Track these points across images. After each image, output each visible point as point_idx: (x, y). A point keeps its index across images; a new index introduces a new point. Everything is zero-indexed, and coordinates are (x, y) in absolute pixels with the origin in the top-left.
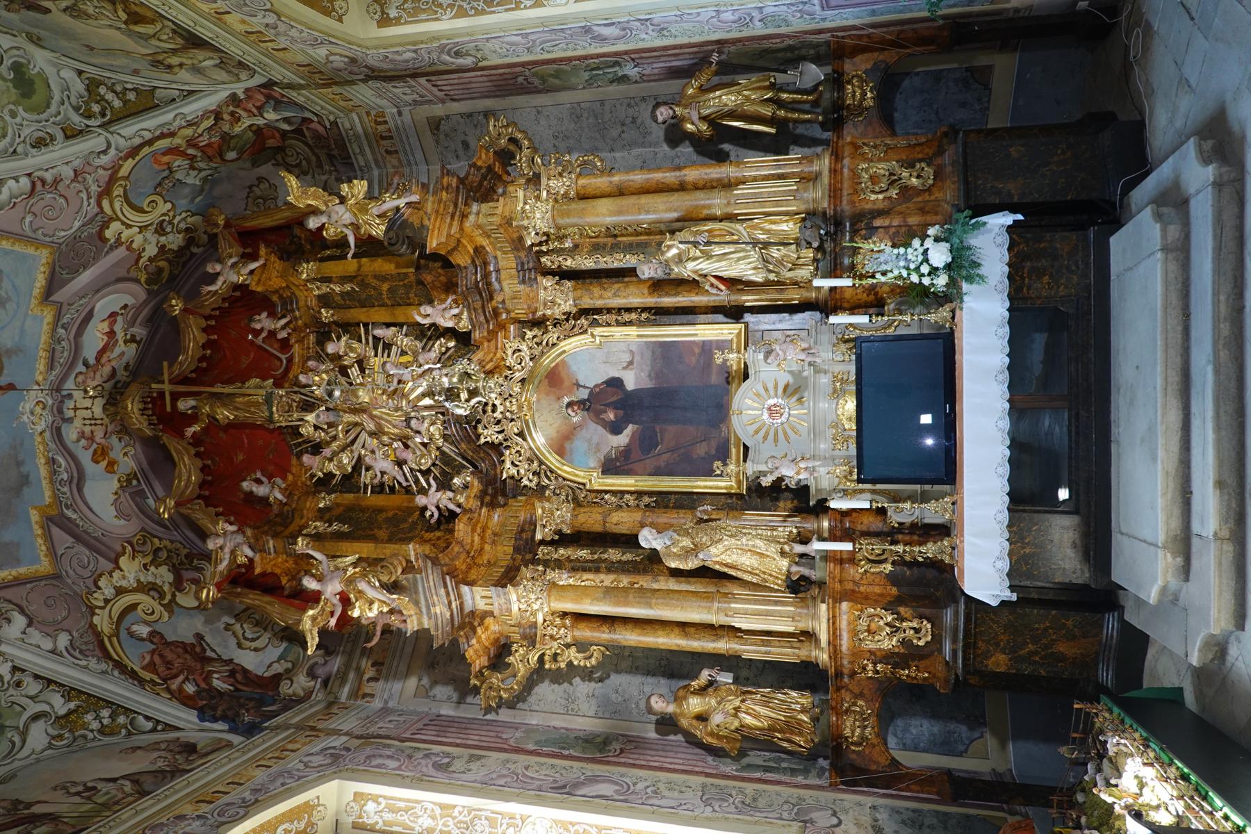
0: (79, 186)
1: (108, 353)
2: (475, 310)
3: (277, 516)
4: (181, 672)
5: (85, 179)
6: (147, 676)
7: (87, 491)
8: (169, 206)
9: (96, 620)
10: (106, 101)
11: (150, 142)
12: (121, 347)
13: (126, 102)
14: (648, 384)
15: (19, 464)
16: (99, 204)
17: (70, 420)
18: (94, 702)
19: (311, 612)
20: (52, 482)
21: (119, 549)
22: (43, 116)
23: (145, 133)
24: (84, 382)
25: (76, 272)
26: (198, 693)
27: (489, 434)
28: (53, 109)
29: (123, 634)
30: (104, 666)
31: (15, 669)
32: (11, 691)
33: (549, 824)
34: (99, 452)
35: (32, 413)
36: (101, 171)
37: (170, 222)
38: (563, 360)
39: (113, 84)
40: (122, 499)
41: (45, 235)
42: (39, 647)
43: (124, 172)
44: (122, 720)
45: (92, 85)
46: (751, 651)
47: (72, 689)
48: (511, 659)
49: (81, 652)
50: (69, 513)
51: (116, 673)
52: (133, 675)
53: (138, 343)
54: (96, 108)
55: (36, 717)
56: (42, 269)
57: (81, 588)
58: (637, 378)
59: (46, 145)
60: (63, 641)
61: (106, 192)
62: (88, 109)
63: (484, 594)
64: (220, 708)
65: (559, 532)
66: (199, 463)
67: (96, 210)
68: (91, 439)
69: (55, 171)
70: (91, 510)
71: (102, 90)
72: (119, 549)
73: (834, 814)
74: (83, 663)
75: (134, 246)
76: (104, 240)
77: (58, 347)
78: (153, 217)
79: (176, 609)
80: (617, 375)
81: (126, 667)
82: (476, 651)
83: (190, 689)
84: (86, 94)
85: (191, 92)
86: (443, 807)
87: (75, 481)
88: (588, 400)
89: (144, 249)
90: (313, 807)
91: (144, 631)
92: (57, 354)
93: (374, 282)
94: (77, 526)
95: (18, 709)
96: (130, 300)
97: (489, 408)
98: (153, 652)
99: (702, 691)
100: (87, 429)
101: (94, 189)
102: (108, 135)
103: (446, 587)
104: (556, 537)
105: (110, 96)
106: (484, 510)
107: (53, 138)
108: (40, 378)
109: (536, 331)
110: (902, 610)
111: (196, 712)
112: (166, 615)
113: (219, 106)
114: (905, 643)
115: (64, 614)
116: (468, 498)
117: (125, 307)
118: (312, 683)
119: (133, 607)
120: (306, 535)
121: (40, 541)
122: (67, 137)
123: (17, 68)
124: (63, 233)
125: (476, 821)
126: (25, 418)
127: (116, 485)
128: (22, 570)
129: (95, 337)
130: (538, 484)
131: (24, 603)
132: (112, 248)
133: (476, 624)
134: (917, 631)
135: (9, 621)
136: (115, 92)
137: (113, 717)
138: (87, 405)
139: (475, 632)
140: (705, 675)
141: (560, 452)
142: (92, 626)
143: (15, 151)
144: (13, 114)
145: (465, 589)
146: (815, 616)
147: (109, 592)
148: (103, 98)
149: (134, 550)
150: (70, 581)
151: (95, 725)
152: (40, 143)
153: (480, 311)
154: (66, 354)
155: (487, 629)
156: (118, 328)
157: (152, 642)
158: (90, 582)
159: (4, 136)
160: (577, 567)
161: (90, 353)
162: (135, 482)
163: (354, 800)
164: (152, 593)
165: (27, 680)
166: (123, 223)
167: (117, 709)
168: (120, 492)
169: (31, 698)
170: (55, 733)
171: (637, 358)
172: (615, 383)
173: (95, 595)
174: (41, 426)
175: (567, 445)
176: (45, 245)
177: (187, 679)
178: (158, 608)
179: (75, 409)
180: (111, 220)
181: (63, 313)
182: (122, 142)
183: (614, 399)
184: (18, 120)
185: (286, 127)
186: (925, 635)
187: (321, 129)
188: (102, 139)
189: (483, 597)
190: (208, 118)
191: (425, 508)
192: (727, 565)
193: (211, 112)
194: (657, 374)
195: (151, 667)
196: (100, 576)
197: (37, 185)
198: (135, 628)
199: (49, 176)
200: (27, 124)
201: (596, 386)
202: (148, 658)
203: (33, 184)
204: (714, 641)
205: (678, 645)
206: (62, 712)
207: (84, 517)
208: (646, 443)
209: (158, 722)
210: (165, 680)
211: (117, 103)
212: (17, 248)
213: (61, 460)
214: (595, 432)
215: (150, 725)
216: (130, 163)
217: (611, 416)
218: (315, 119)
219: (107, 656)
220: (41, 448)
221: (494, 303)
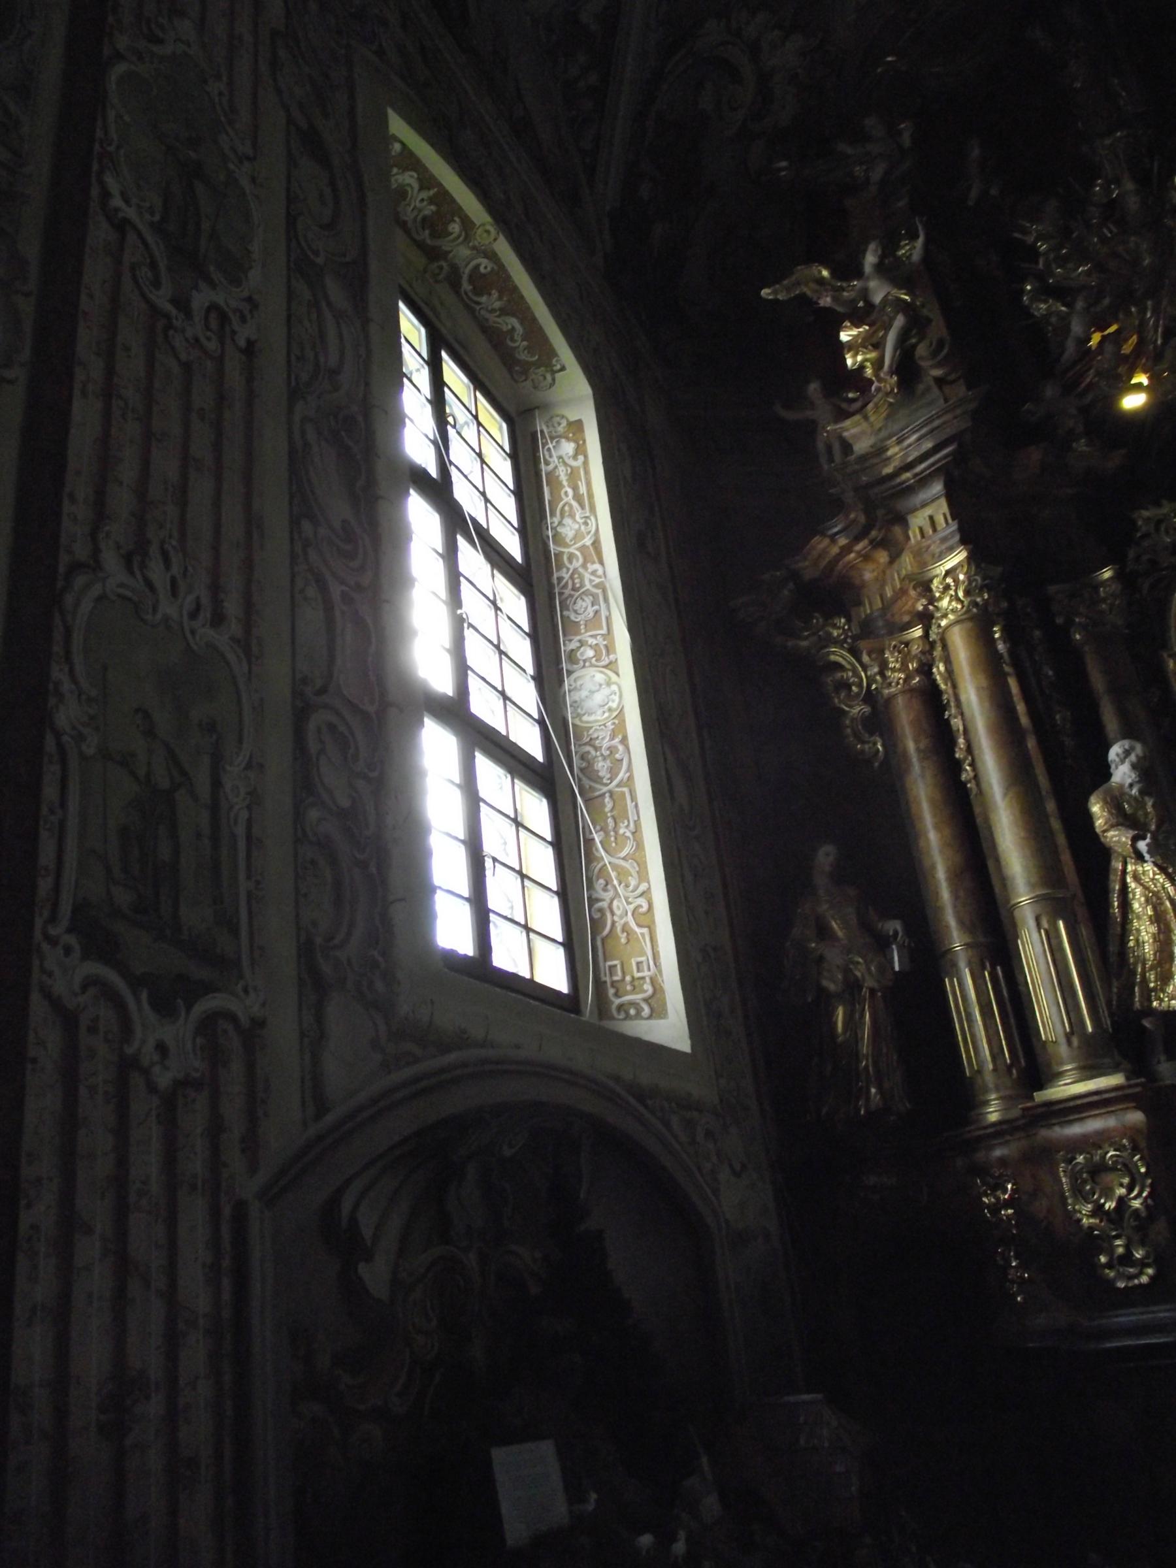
19: (825, 273)
33: (614, 705)
46: (966, 988)
48: (817, 620)
63: (940, 520)
73: (744, 1166)
82: (825, 552)
86: (596, 544)
90: (549, 366)
99: (866, 926)
110: (1161, 1227)
114: (1093, 1242)
125: (588, 600)
133: (874, 533)
134: (1127, 1259)
139: (857, 539)
140: (894, 926)
145: (937, 488)
146: (1089, 1070)
155: (867, 558)
163: (570, 424)
186: (1121, 1276)
189: (931, 518)
192: (1125, 905)
204: (961, 922)
205: (933, 867)
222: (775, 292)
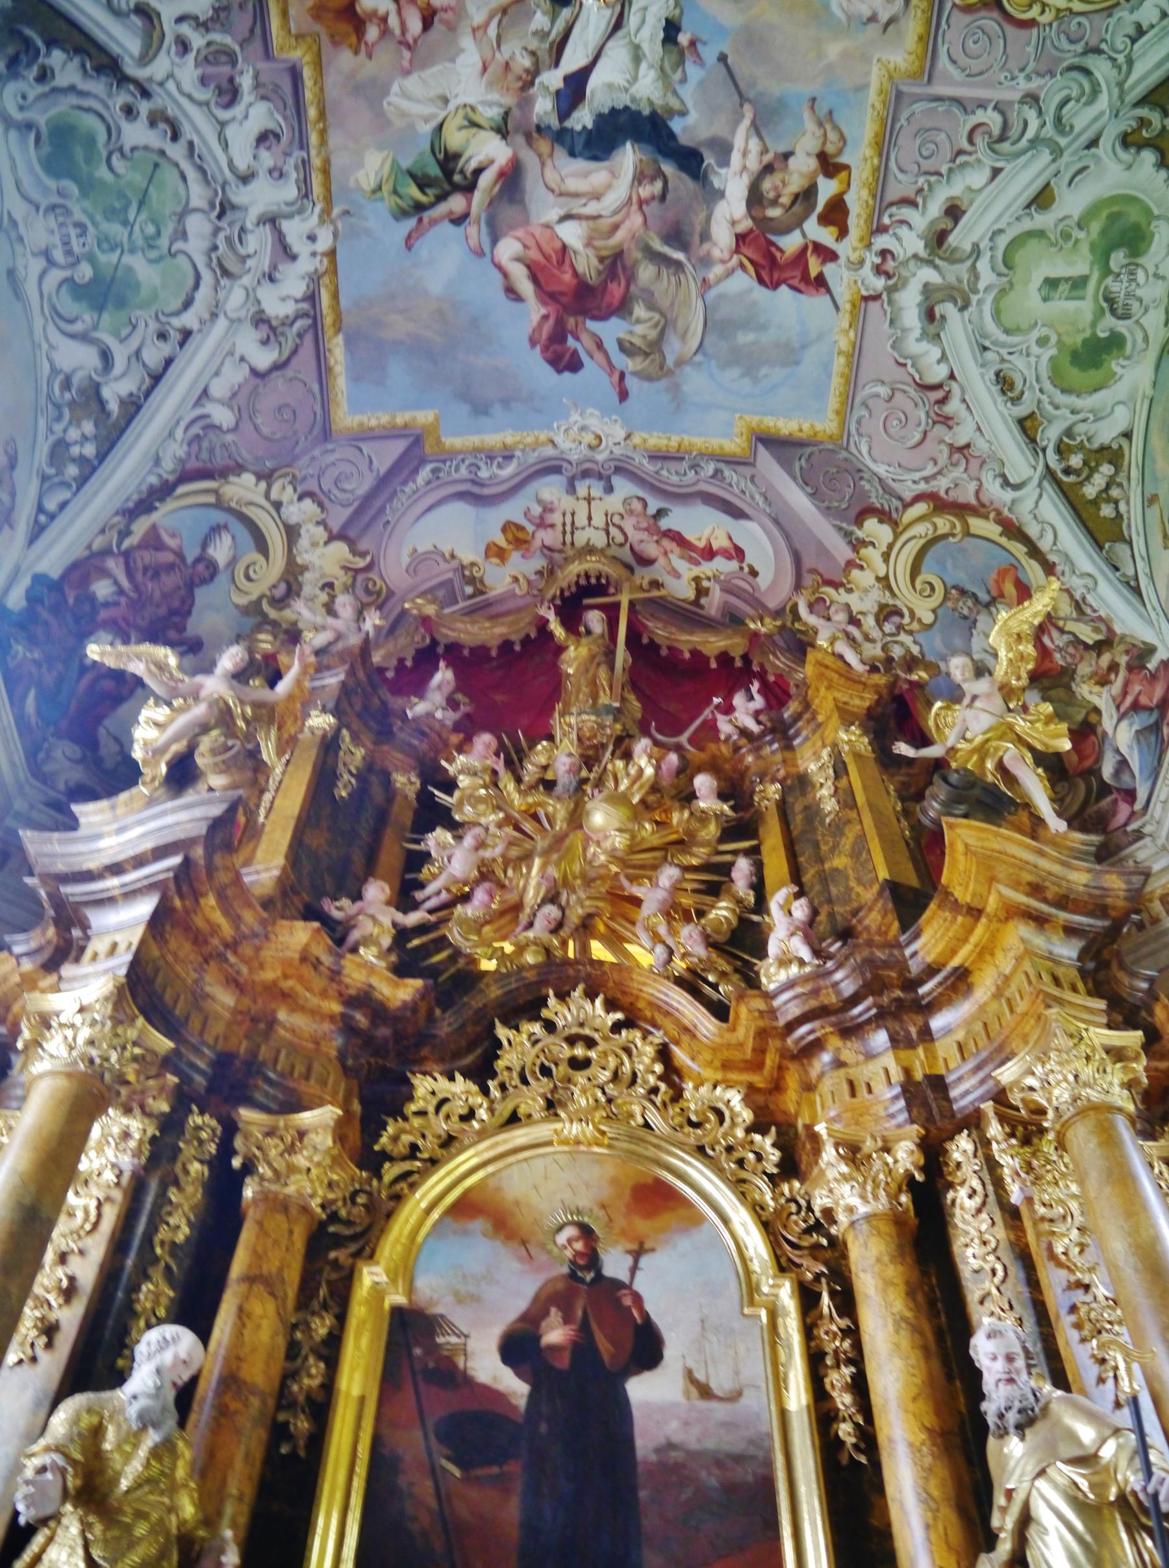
0: (943, 459)
1: (677, 550)
2: (815, 992)
3: (384, 703)
4: (136, 587)
5: (955, 465)
6: (141, 527)
7: (460, 508)
8: (928, 618)
9: (248, 478)
10: (1088, 478)
11: (1034, 552)
12: (688, 571)
13: (1095, 503)
14: (645, 1444)
15: (506, 402)
16: (918, 498)
17: (571, 489)
18: (111, 437)
19: (173, 661)
20: (476, 451)
21: (363, 545)
22: (1047, 385)
23: (1049, 536)
24: (631, 512)
25: (805, 481)
26: (92, 599)
27: (518, 1045)
28: (1061, 398)
29: (219, 517)
30: (168, 465)
31: (186, 334)
32: (153, 326)
34: (520, 535)
35: (583, 428)
36: (972, 487)
37: (900, 628)
38: (698, 1219)
39: (1120, 485)
40: (444, 566)
41: (859, 422)
42: (217, 374)
43: (977, 525)
44: (72, 470)
45: (1112, 455)
47: (139, 408)
49: (198, 437)
50: (425, 473)
51: (153, 480)
52: (145, 505)
53: (696, 603)
54: (1076, 461)
55: (106, 357)
56: (806, 426)
57: (302, 467)
58: (666, 1410)
59: (1003, 392)
60: (223, 416)
61: (940, 505)
62: (1071, 450)
64: (52, 621)
65: (249, 1168)
66: (494, 644)
67: (908, 496)
68: (542, 524)
69: (964, 413)
70: (430, 509)
71: (1107, 469)
72: (363, 545)
74: (179, 433)
75: (855, 573)
76: (859, 520)
77: (685, 465)
78: (906, 596)
79: (251, 621)
80: (671, 1352)
81: (162, 500)
83: (102, 589)
84: (1096, 445)
85: (1137, 591)
87: (476, 490)
88: (599, 1276)
89: (850, 591)
91: (220, 552)
92: (673, 466)
93: (847, 842)
94: (405, 483)
95: (125, 332)
96: (764, 581)
97: (579, 1051)
98: (180, 555)
100: (556, 518)
101: (941, 485)
102: (1036, 481)
103: (160, 853)
104: (236, 1163)
105: (1099, 480)
106: (336, 1008)
107: (1016, 401)
108: (636, 439)
109: (774, 1155)
111: (55, 574)
112: (243, 601)
113: (1123, 638)
115: (266, 430)
116: (371, 969)
117: (754, 573)
118: (61, 786)
119: (262, 546)
120: (337, 732)
121: (385, 419)
122: (1021, 422)
123: (1115, 342)
124: (864, 449)
126: (575, 417)
127: (467, 557)
128: (341, 382)
129: (701, 524)
130: (385, 1156)
131: (289, 372)
132: (847, 535)
135: (265, 342)
136: (1108, 486)
137: (82, 460)
138: (595, 518)
141: (466, 1208)
142: (239, 469)
143: (985, 349)
144: (1042, 342)
148: (1093, 471)
149: (357, 571)
150: (317, 452)
151: (73, 434)
152: (1004, 383)
153: (813, 1003)
154: (675, 479)
156: (721, 565)
157: (198, 560)
158: (312, 485)
159: (1007, 332)
160: (140, 1195)
161: (679, 519)
162: (469, 590)
164: (283, 587)
165: (166, 349)
166: (890, 547)
167: (89, 469)
168: (455, 564)
169: (138, 353)
170: (75, 381)
171: (719, 1410)
172: (646, 1349)
173: (290, 489)
174: (564, 443)
175: (479, 1225)
176: (843, 424)
177: (121, 592)
178: (255, 591)
179: (589, 500)
180: (894, 524)
181: (740, 469)
182: (1029, 504)
183: (604, 1345)
184: (1035, 350)
185: (1107, 771)
187: (1121, 817)
188: (1030, 472)
190: (1097, 630)
191: (357, 896)
193: (1110, 630)
194: (675, 1467)
195: (153, 541)
196: (321, 505)
197: (937, 392)
198: (226, 539)
199: (954, 406)
200: (1031, 364)
201: (638, 1299)
202: (171, 542)
203: (938, 387)
206: (106, 393)
207: (417, 495)
208: (476, 1428)
209: (52, 517)
210: (127, 555)
211: (1090, 491)
212: (836, 382)
213: (510, 469)
214: (512, 1289)
215: (51, 505)
216: (991, 529)
217: (555, 1334)
218: (1138, 806)
219: (186, 477)
220: (530, 440)
221: (835, 1042)
222: (102, 654)
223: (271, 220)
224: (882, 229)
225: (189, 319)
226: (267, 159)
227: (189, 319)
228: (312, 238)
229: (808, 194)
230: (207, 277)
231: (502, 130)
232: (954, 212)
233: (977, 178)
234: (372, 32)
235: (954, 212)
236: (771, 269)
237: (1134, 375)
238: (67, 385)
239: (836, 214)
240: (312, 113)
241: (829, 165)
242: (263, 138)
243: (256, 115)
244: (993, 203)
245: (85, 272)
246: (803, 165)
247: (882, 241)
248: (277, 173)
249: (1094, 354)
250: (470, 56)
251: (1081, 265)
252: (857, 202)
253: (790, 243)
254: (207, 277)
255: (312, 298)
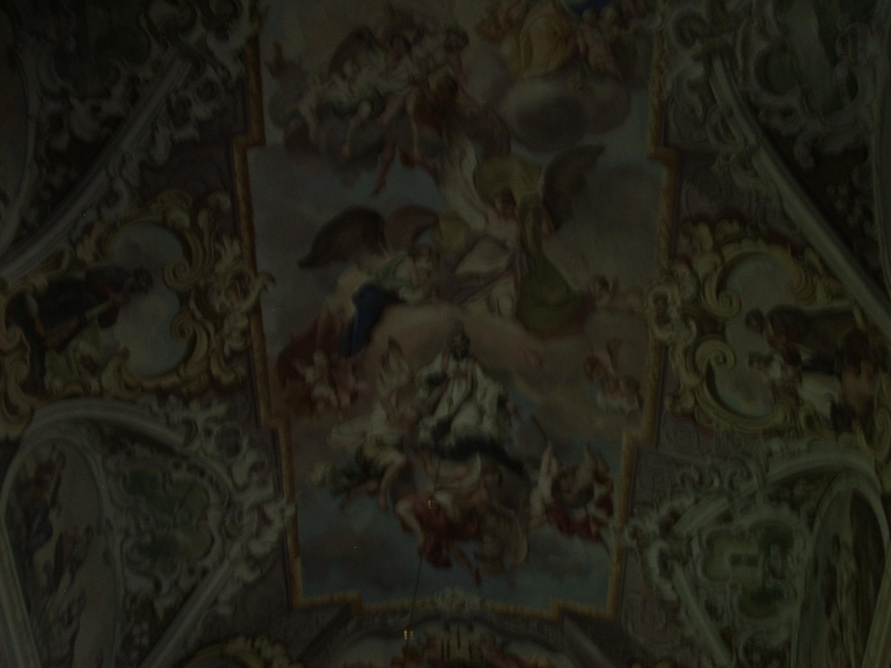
17: (447, 628)
44: (134, 655)
55: (158, 585)
60: (224, 610)
128: (299, 581)
147: (268, 652)
152: (711, 610)
199: (682, 615)
223: (259, 508)
224: (632, 515)
225: (208, 562)
226: (255, 478)
227: (208, 562)
228: (282, 511)
229: (588, 493)
230: (218, 539)
231: (400, 447)
232: (675, 516)
233: (687, 501)
234: (320, 407)
235: (675, 516)
236: (567, 526)
237: (790, 612)
238: (134, 600)
239: (606, 504)
240: (283, 449)
241: (600, 478)
242: (254, 468)
243: (250, 457)
244: (700, 516)
245: (148, 539)
246: (584, 476)
247: (634, 522)
248: (263, 483)
249: (764, 600)
250: (379, 413)
251: (753, 550)
252: (618, 500)
253: (579, 515)
254: (218, 539)
255: (282, 540)
